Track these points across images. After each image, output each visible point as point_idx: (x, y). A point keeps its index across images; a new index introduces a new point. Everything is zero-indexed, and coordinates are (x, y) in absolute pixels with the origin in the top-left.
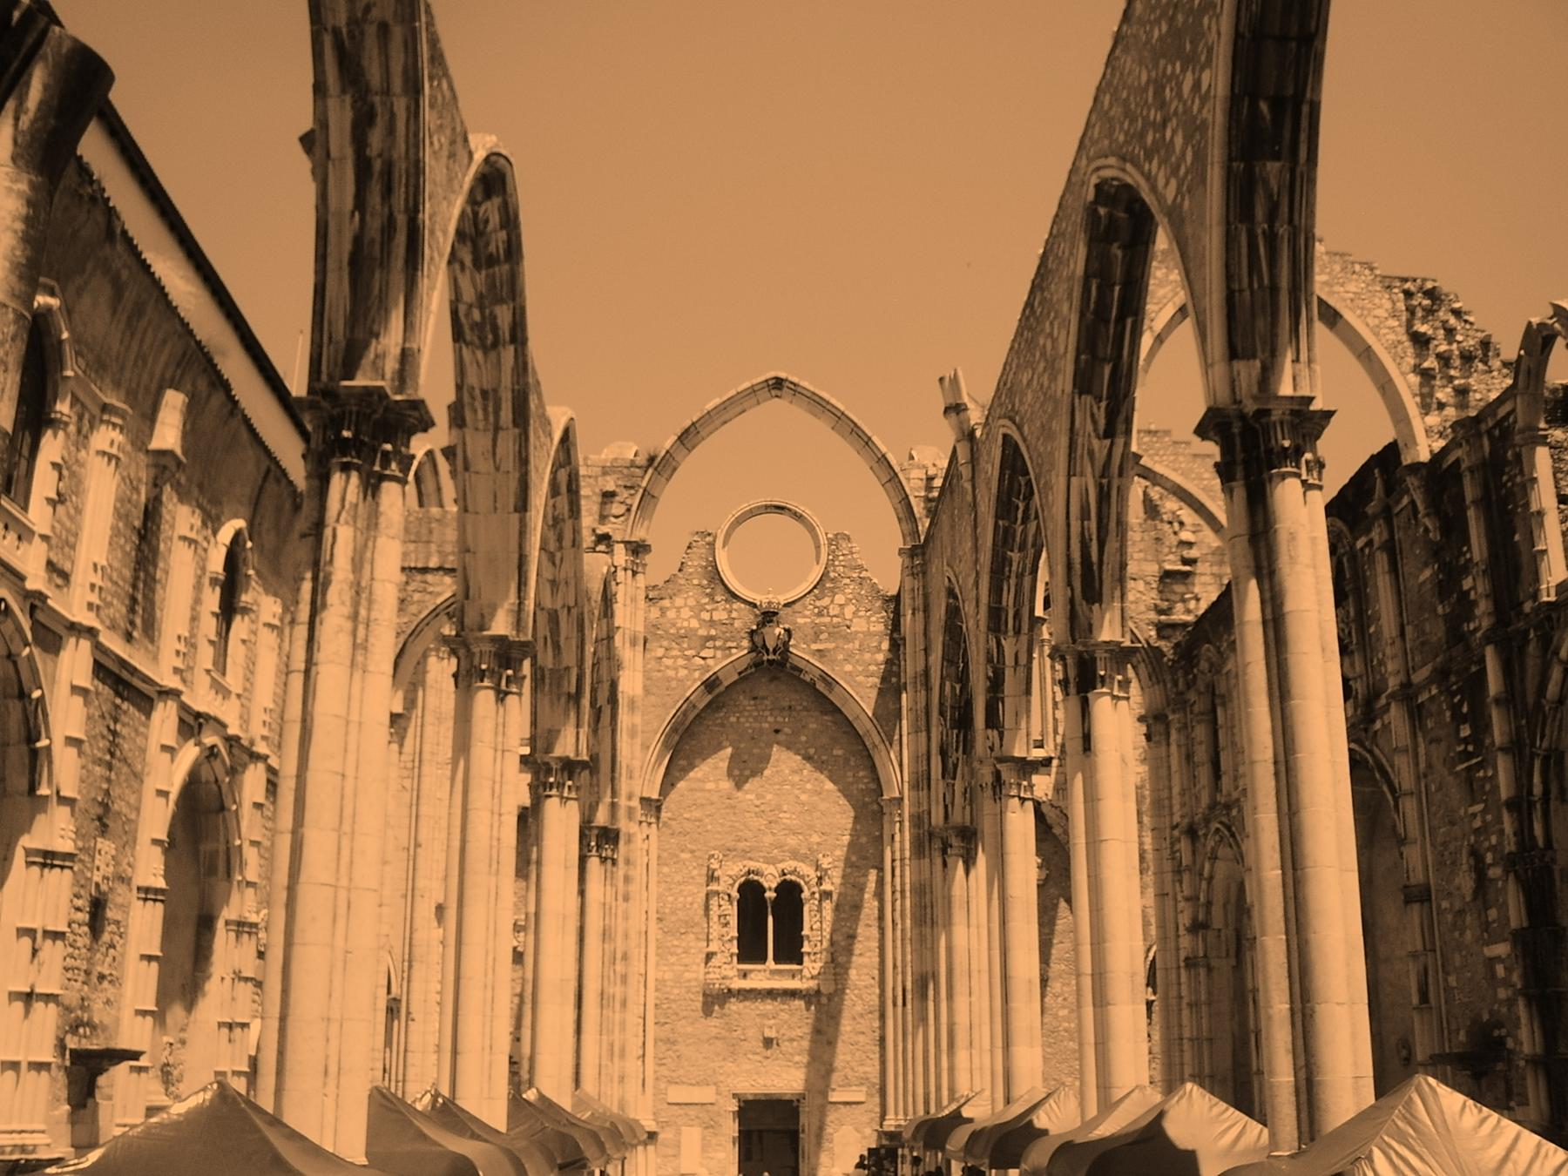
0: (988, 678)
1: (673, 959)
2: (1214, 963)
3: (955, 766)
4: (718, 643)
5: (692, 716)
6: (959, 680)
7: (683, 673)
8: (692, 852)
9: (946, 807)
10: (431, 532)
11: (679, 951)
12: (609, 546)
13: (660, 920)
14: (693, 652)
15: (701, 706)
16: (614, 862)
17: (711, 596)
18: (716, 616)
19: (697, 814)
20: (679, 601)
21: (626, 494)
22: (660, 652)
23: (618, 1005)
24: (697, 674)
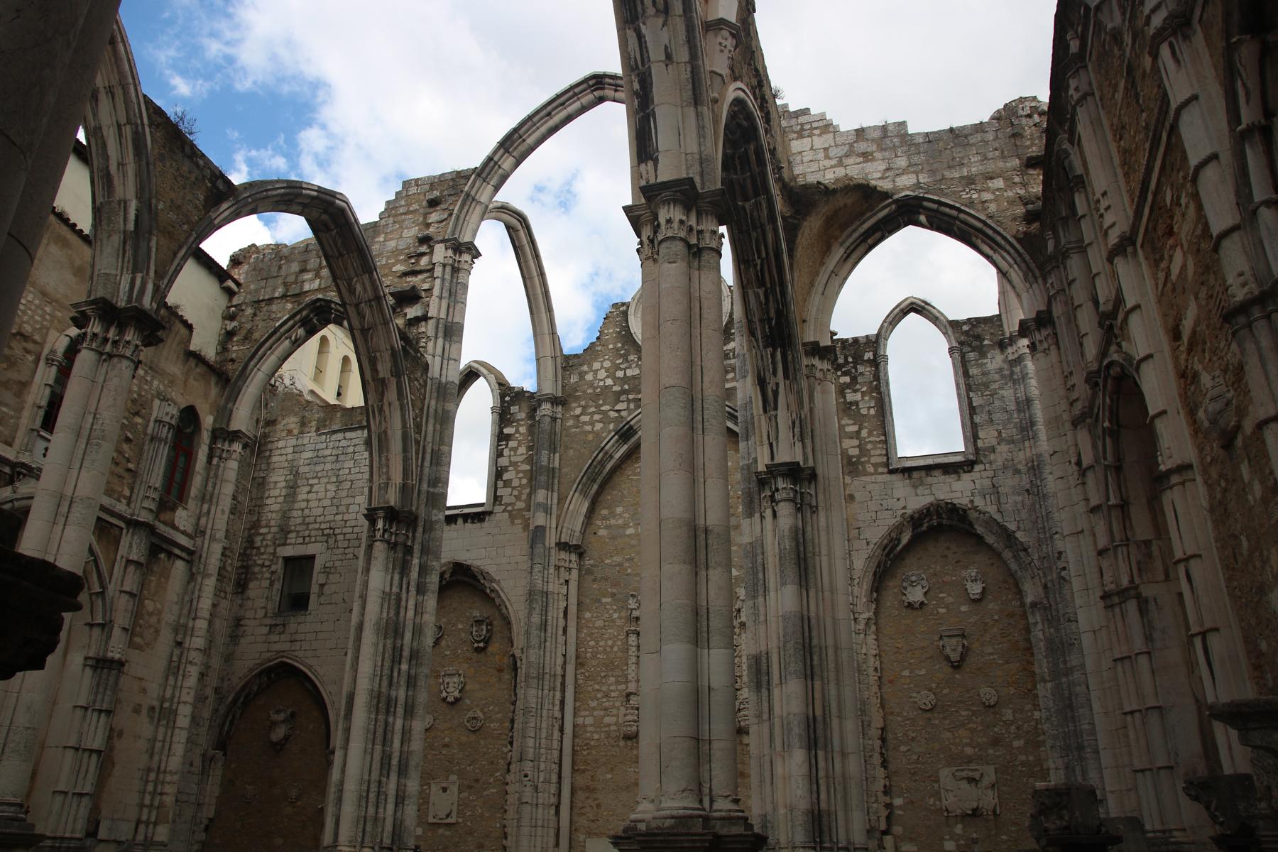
0: (636, 93)
1: (594, 704)
2: (1146, 591)
3: (776, 393)
4: (631, 397)
5: (609, 466)
6: (761, 283)
7: (598, 426)
8: (613, 595)
9: (771, 445)
10: (280, 267)
11: (599, 696)
12: (431, 248)
13: (580, 664)
14: (608, 407)
15: (617, 456)
16: (409, 551)
17: (625, 357)
18: (629, 373)
19: (617, 559)
20: (596, 365)
21: (451, 200)
22: (578, 411)
23: (400, 710)
24: (611, 426)
